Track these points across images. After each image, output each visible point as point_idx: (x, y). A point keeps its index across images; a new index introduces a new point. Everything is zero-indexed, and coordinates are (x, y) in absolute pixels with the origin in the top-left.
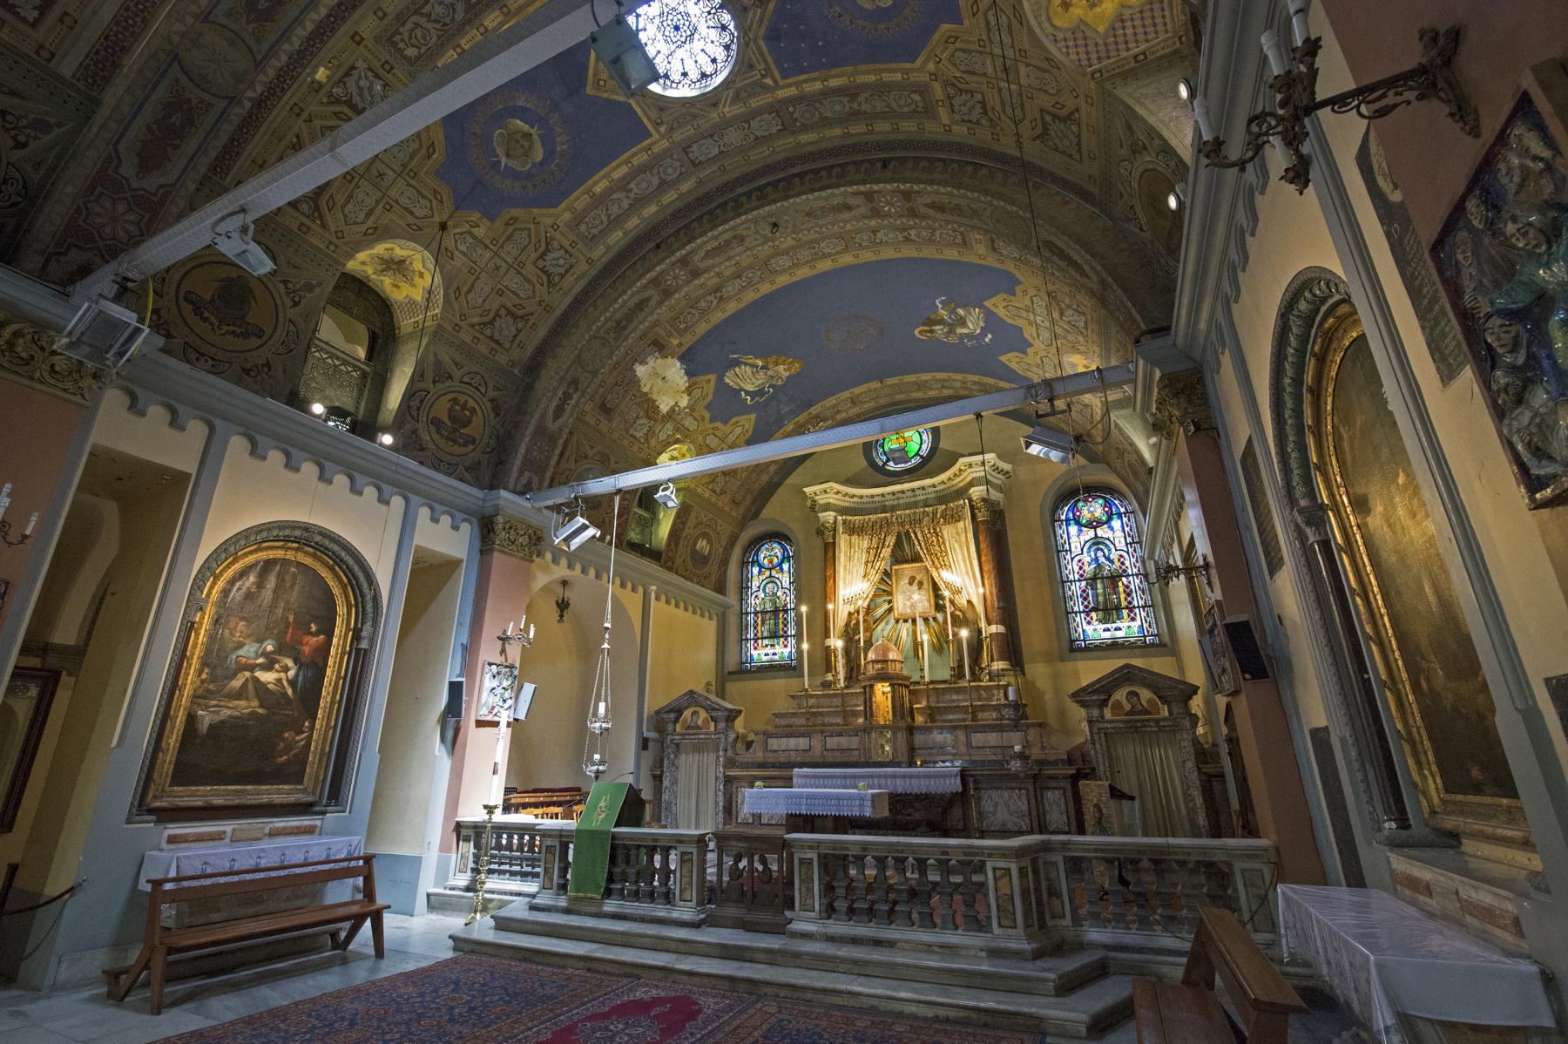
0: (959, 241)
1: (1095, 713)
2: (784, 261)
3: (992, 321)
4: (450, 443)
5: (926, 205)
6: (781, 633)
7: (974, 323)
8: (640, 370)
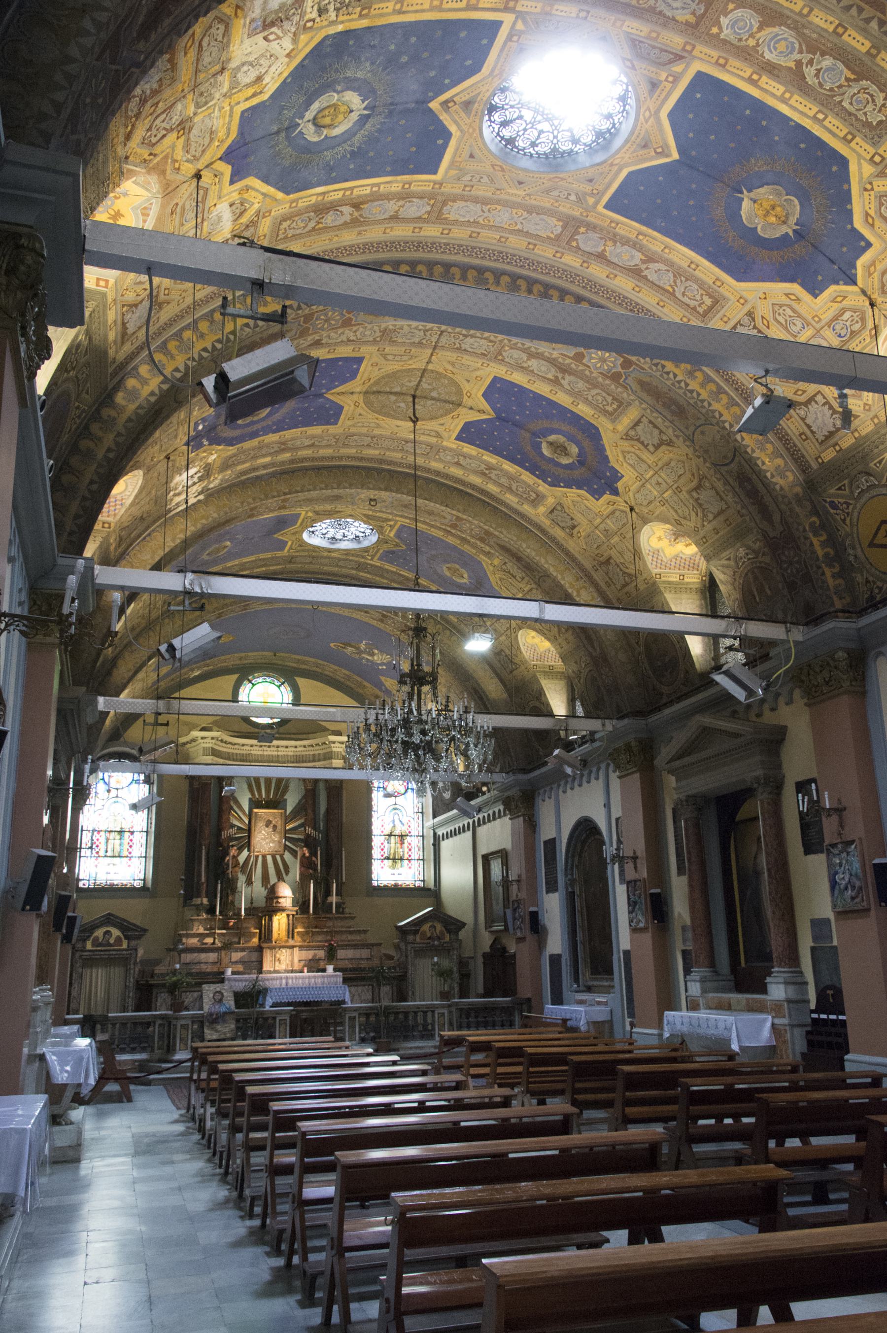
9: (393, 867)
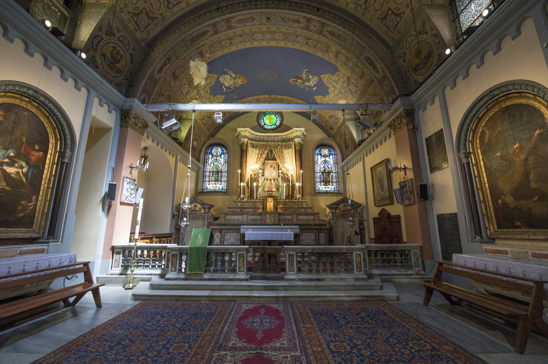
0: (325, 50)
1: (334, 211)
2: (259, 36)
3: (320, 84)
4: (110, 69)
5: (328, 31)
6: (219, 180)
7: (313, 81)
8: (192, 63)
9: (325, 185)
